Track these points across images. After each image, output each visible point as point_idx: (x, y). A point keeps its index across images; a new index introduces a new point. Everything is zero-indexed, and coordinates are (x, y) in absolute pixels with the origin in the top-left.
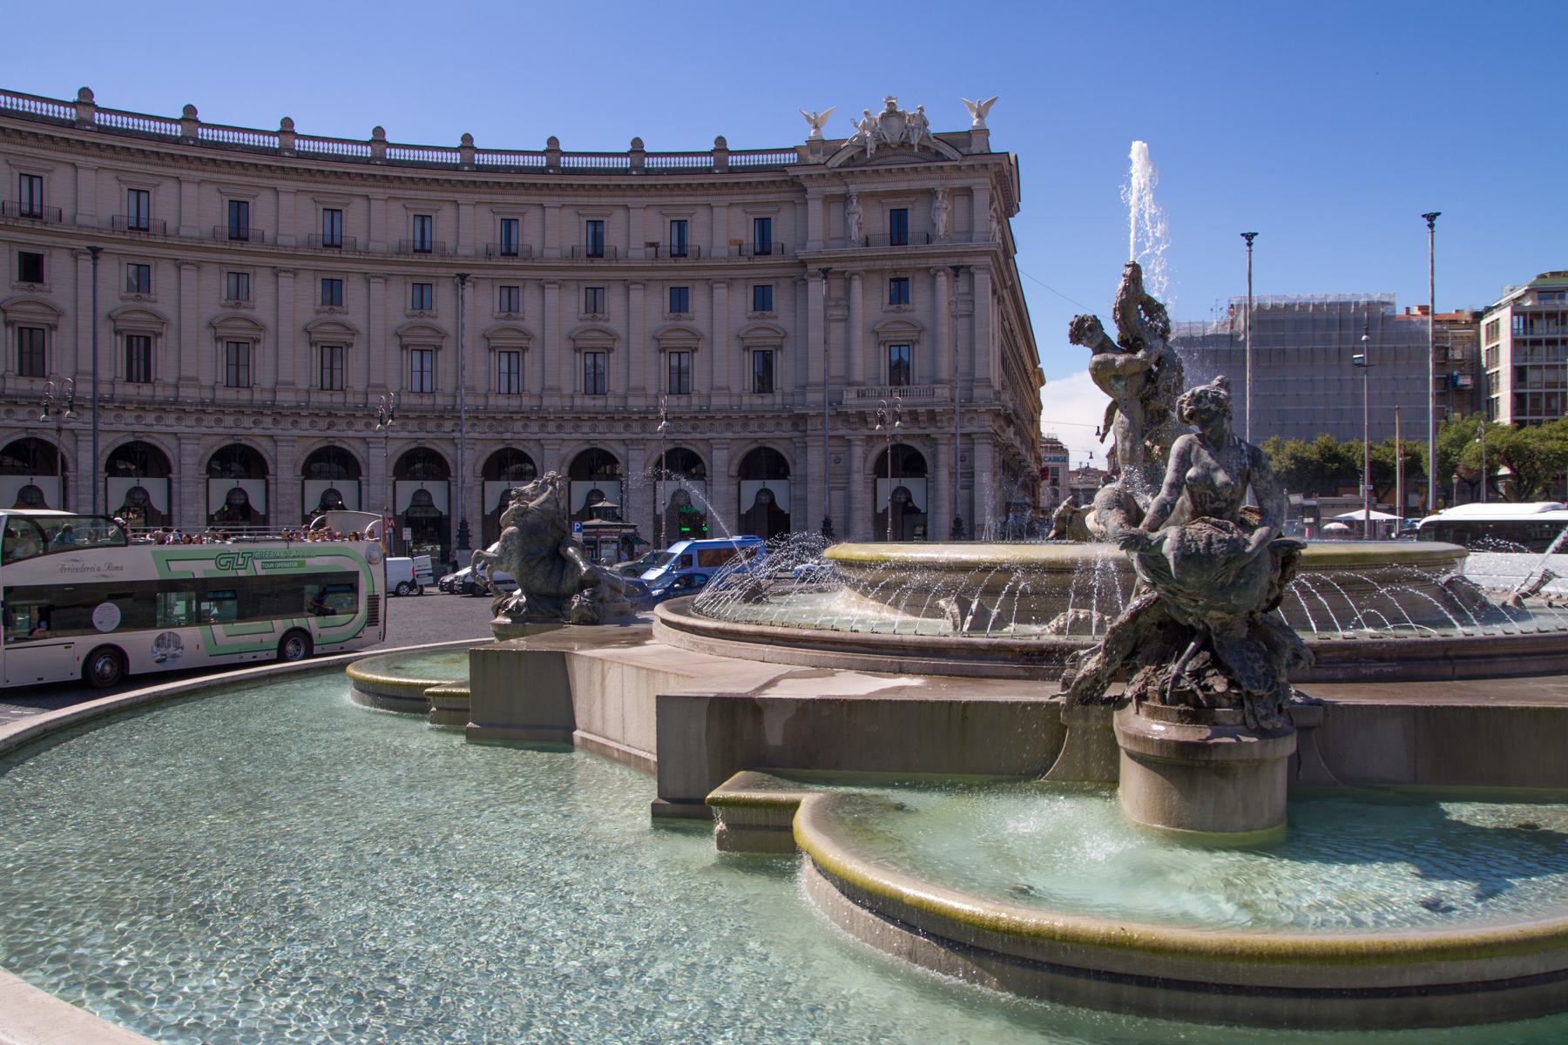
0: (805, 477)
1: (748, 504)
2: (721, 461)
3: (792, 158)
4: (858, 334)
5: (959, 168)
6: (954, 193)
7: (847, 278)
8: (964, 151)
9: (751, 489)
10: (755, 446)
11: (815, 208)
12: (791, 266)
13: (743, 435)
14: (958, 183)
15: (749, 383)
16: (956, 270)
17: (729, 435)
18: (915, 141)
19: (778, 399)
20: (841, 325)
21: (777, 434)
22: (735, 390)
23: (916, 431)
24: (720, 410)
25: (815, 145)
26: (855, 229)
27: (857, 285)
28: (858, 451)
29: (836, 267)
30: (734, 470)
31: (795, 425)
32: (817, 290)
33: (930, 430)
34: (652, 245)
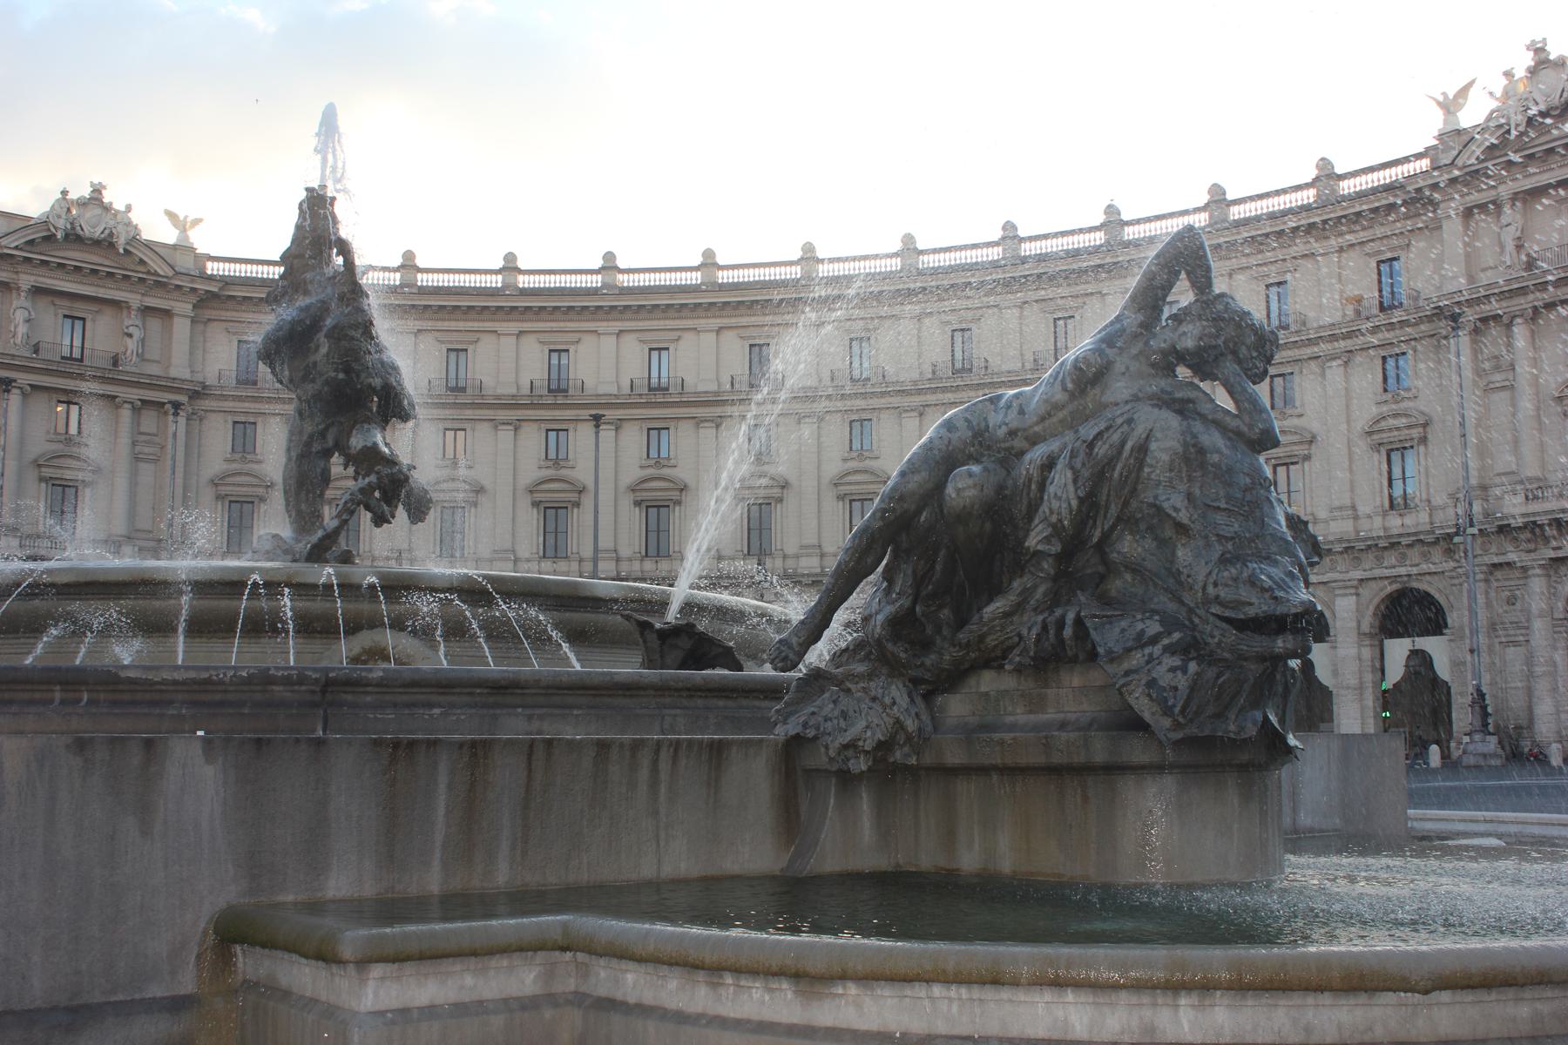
0: (1462, 628)
1: (1395, 671)
2: (1348, 613)
3: (1424, 164)
7: (1509, 325)
9: (1398, 651)
10: (1395, 587)
11: (1453, 227)
12: (1430, 319)
13: (1377, 572)
17: (1357, 574)
19: (1423, 517)
20: (1505, 395)
21: (1425, 567)
22: (1363, 509)
24: (1340, 541)
25: (1455, 137)
26: (1510, 246)
27: (1520, 332)
30: (1366, 628)
31: (1449, 552)
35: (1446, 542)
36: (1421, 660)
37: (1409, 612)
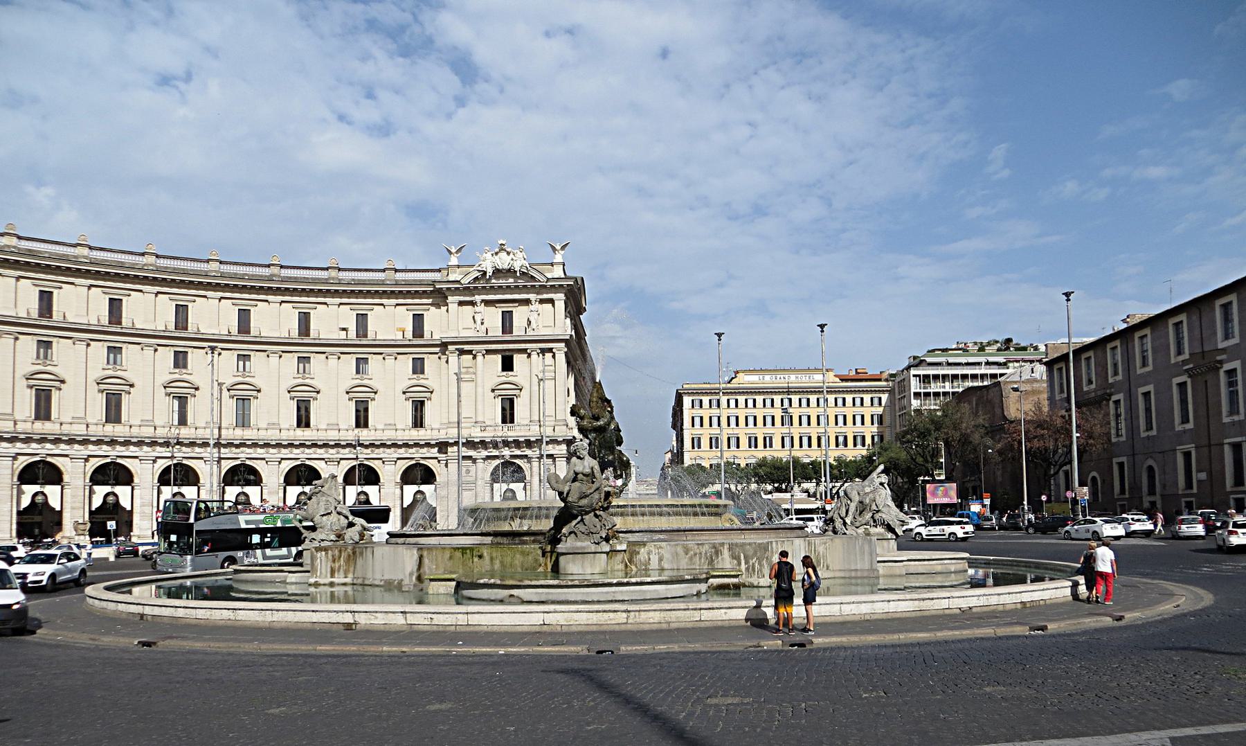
4: (480, 390)
5: (545, 286)
6: (542, 301)
8: (549, 276)
11: (453, 307)
14: (545, 296)
15: (410, 422)
16: (543, 351)
18: (517, 269)
23: (518, 452)
27: (480, 357)
28: (480, 464)
29: (466, 347)
32: (453, 358)
33: (528, 452)
34: (344, 329)
35: (443, 446)
36: (419, 498)
37: (419, 474)
